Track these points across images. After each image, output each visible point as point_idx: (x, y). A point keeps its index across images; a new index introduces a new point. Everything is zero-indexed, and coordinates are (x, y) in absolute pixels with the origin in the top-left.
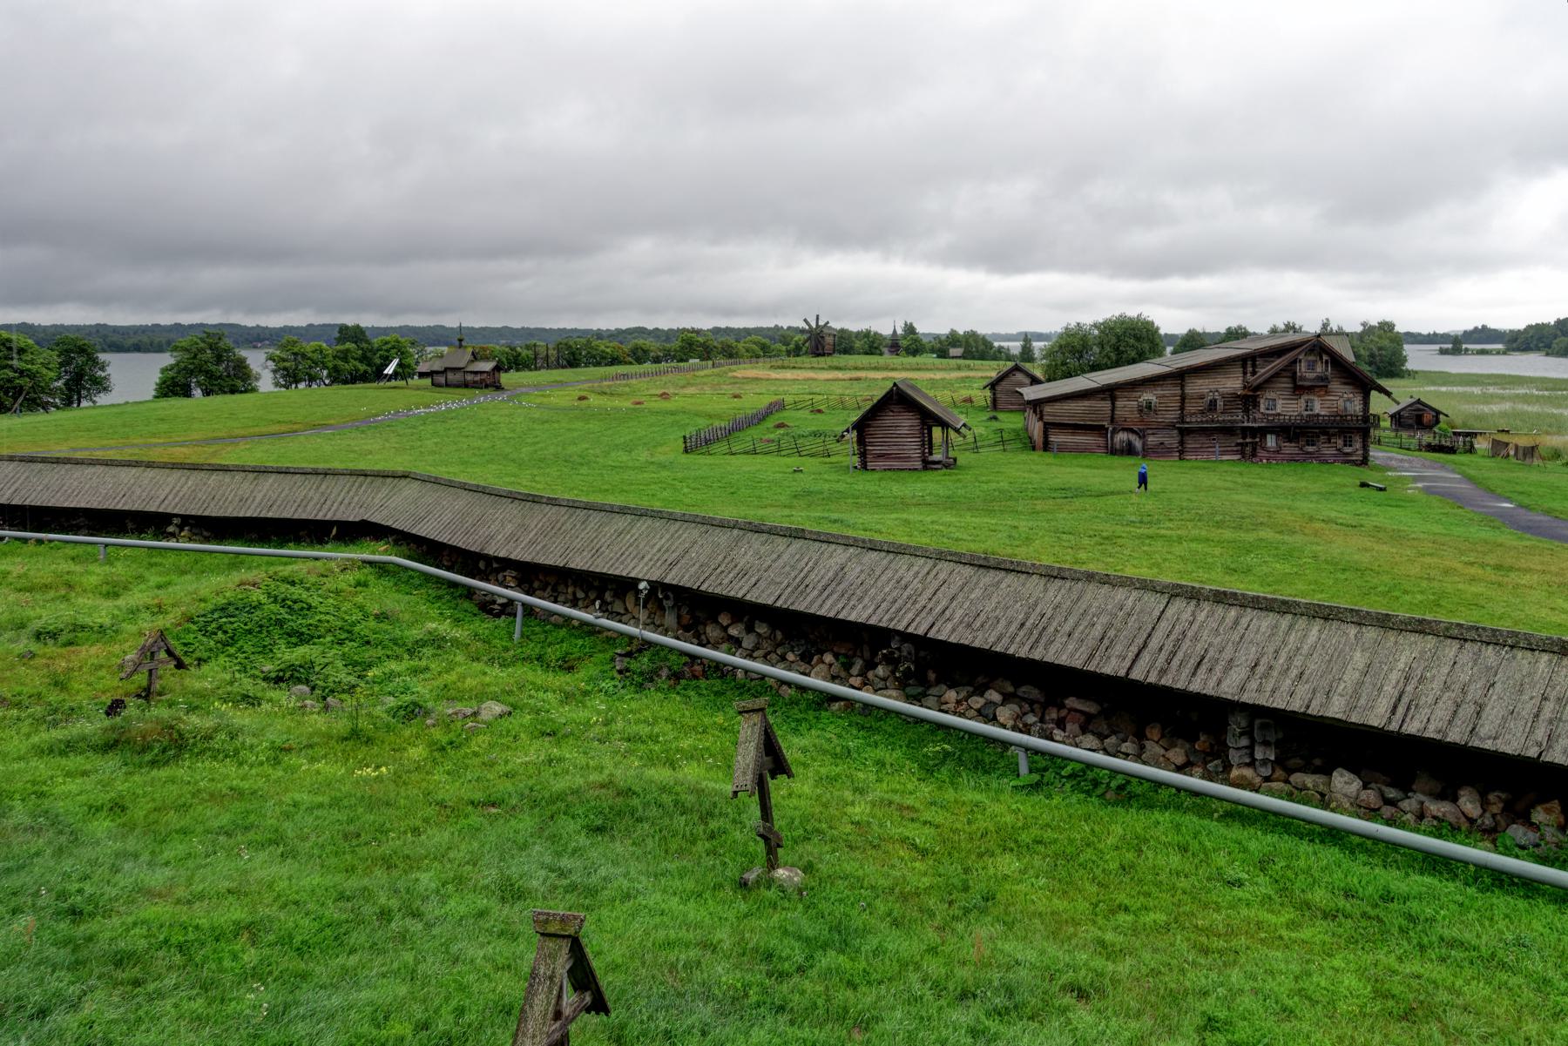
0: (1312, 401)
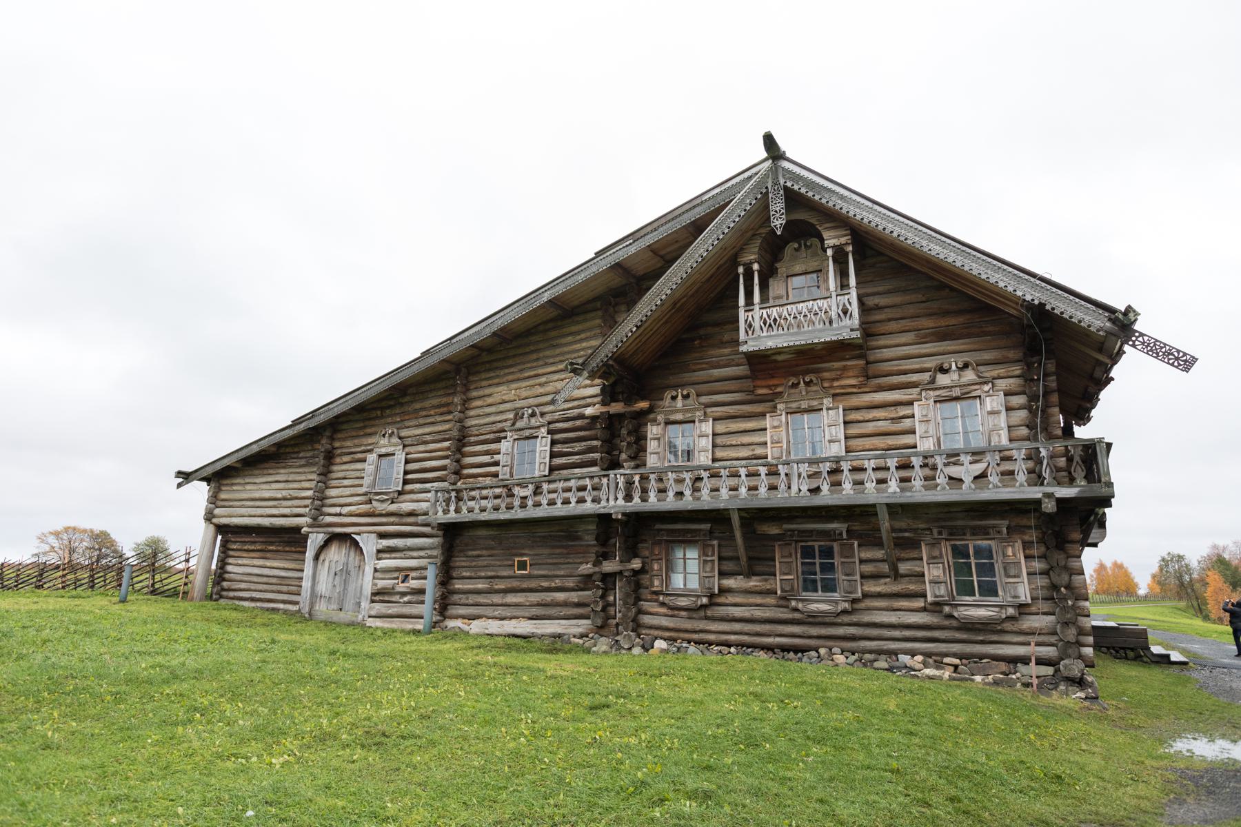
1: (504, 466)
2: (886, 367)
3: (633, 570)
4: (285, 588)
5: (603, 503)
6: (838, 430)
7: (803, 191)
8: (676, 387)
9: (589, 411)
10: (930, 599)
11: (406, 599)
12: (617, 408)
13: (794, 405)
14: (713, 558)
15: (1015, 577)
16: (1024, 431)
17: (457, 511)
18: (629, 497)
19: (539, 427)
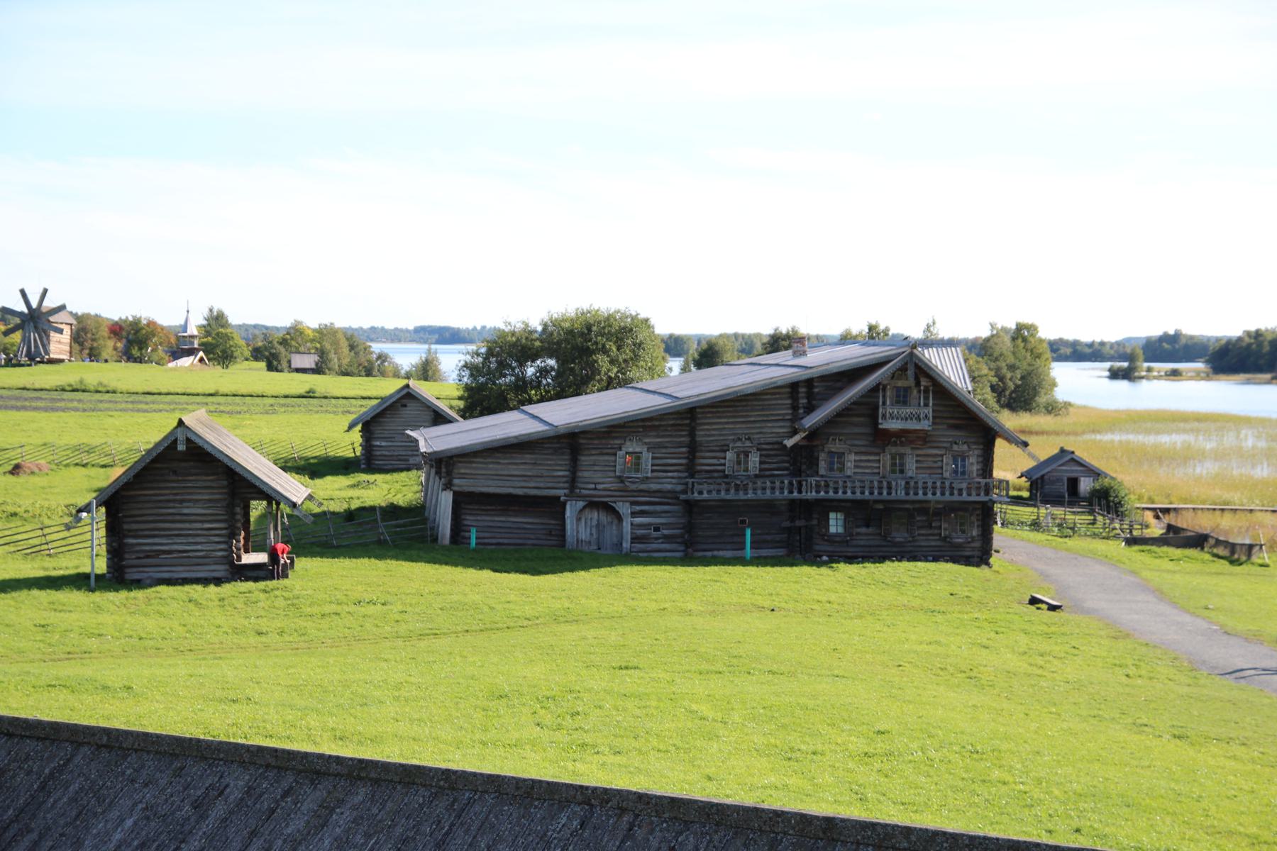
0: (902, 456)
2: (934, 439)
4: (532, 537)
5: (804, 494)
8: (835, 434)
10: (943, 535)
11: (660, 541)
18: (818, 492)
19: (751, 447)
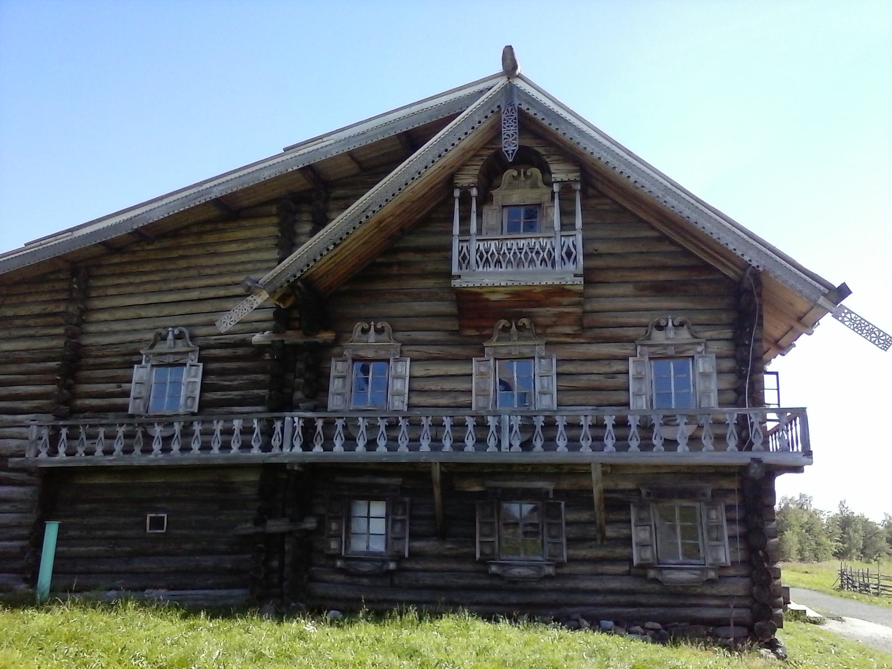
1: (135, 398)
3: (306, 530)
5: (276, 450)
6: (550, 381)
7: (539, 117)
8: (368, 319)
9: (257, 338)
10: (636, 561)
12: (293, 337)
13: (504, 351)
14: (404, 517)
15: (717, 539)
16: (731, 396)
17: (70, 453)
18: (307, 446)
19: (187, 353)
